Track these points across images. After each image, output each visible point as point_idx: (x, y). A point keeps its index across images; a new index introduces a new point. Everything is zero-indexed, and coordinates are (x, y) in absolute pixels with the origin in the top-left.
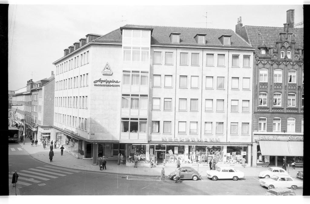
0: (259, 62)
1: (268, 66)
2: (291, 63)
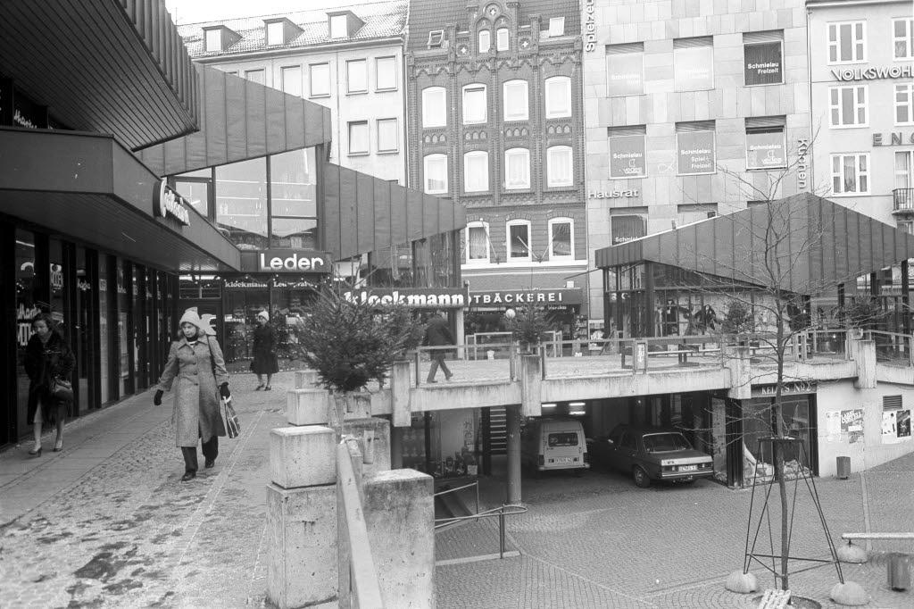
0: (418, 71)
1: (443, 78)
2: (509, 62)
